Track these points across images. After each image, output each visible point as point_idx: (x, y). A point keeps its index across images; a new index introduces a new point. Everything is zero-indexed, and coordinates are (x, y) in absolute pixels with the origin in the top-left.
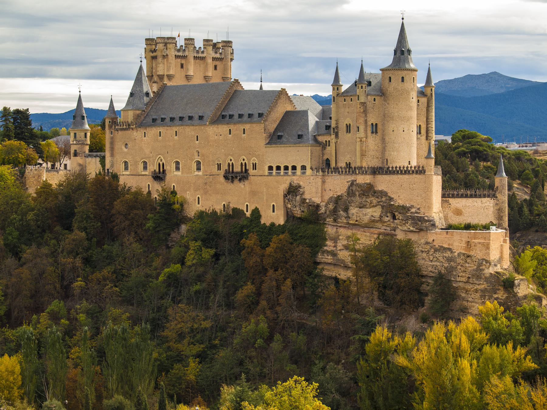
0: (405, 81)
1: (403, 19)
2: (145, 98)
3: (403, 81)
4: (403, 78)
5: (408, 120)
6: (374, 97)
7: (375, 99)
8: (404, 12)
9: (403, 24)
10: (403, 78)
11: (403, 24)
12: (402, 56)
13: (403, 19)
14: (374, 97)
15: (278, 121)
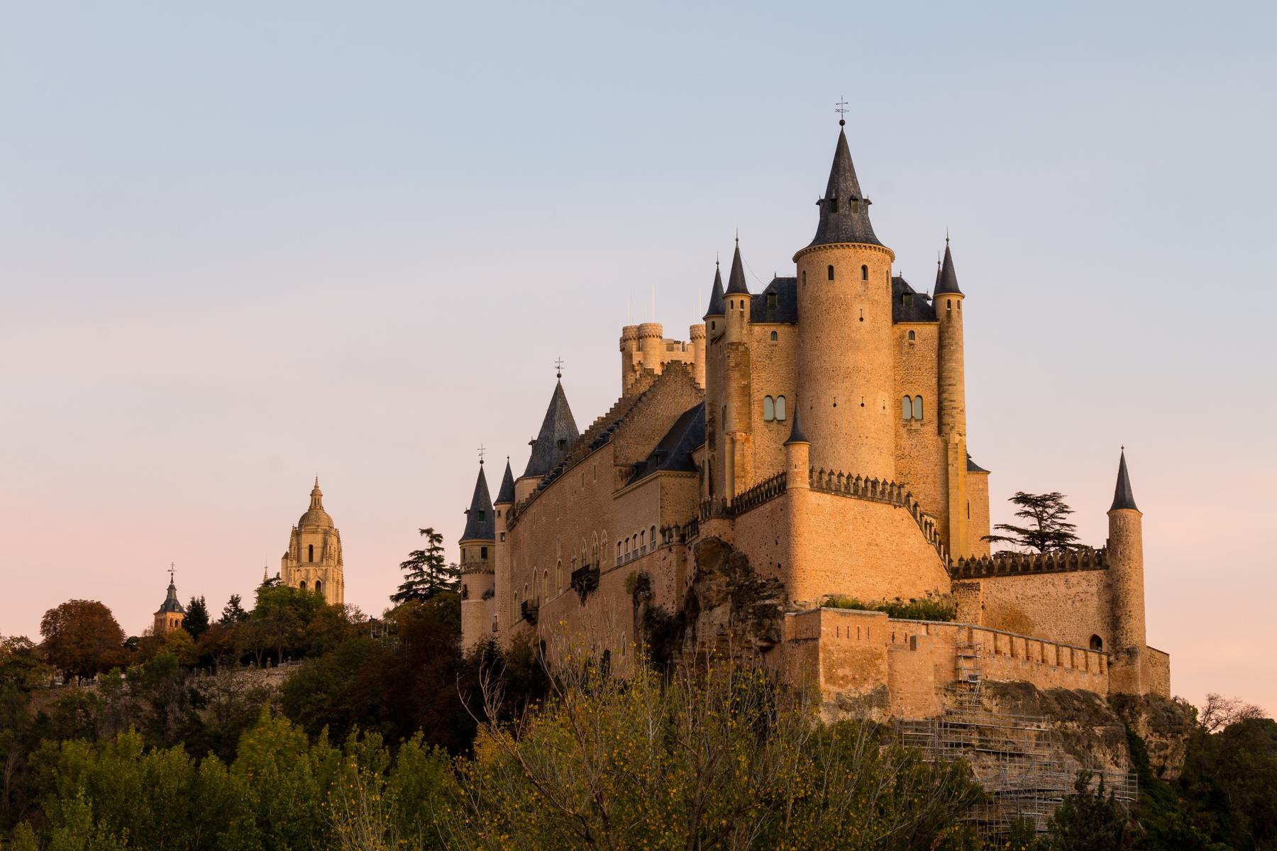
0: (836, 276)
1: (842, 123)
2: (555, 451)
3: (831, 277)
4: (831, 268)
5: (847, 376)
6: (774, 329)
7: (774, 333)
8: (845, 107)
9: (842, 136)
10: (831, 268)
11: (842, 136)
12: (833, 215)
13: (842, 123)
14: (774, 329)
15: (658, 439)
